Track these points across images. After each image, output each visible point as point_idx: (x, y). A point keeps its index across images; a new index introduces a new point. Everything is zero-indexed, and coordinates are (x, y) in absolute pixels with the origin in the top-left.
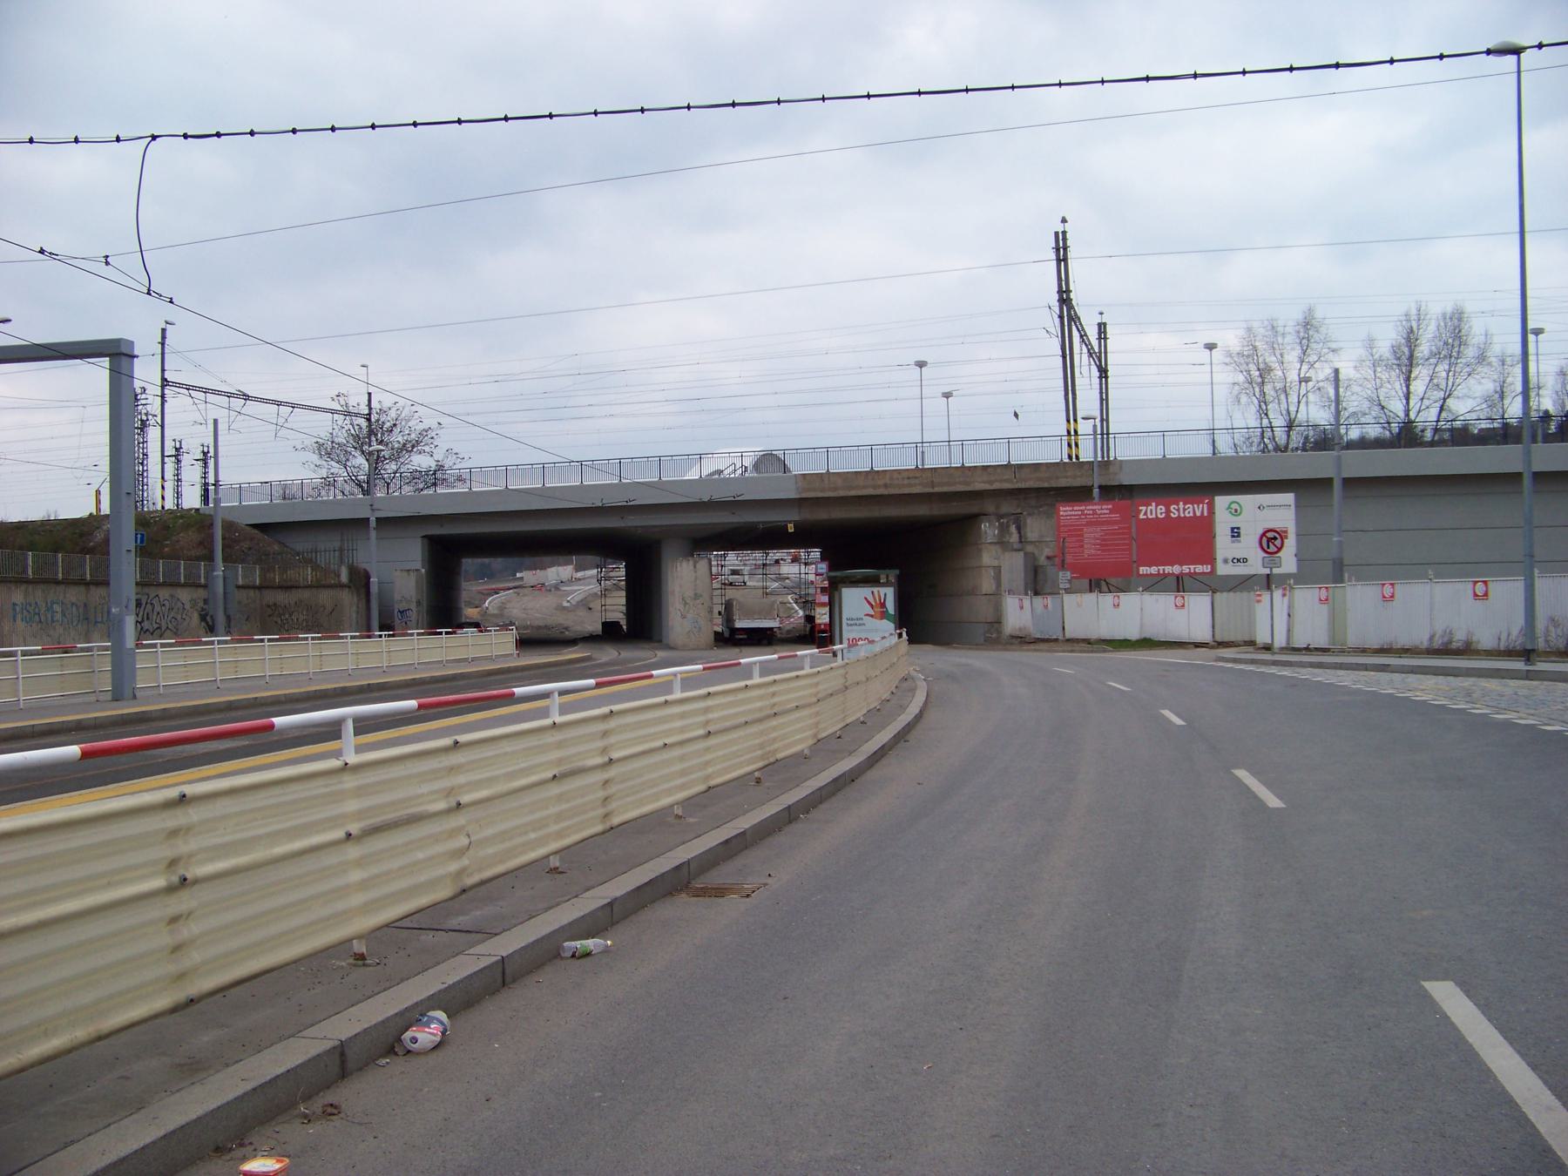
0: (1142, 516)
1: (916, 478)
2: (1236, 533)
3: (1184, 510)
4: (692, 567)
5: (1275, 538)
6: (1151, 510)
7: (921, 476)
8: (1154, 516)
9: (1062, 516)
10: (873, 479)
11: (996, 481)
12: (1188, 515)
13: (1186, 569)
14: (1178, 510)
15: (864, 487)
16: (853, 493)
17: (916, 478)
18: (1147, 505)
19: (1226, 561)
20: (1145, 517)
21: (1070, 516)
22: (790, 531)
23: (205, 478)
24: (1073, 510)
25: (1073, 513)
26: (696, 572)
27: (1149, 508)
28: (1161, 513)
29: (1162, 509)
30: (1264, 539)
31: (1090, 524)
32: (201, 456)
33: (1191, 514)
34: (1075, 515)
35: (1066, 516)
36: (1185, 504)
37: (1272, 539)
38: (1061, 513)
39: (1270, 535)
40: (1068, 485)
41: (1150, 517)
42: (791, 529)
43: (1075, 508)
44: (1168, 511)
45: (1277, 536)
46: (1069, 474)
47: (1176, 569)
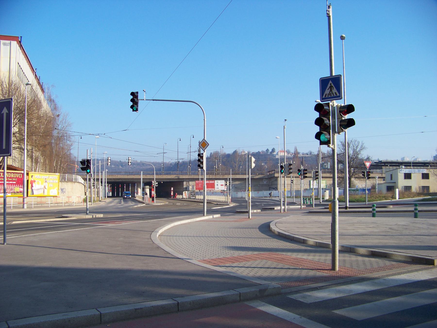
2: (217, 185)
13: (211, 189)
19: (216, 188)
31: (200, 183)
42: (162, 183)
44: (209, 182)
47: (210, 189)
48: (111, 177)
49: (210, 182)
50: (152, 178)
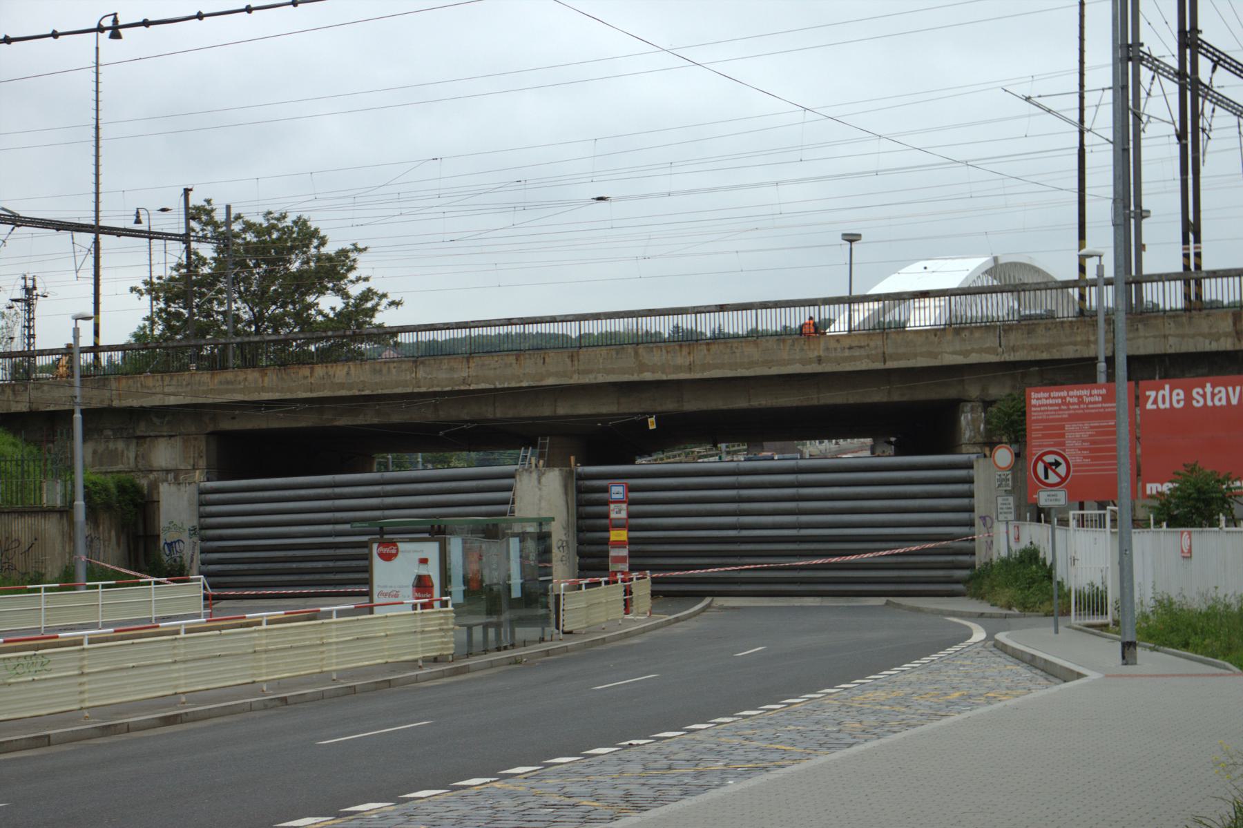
0: (1149, 406)
1: (860, 347)
3: (1213, 395)
4: (536, 483)
5: (1057, 464)
6: (1164, 396)
7: (868, 345)
8: (1167, 405)
9: (1035, 406)
10: (802, 350)
11: (973, 351)
12: (1217, 403)
14: (1204, 396)
15: (790, 362)
16: (775, 371)
17: (860, 347)
18: (1158, 388)
20: (1154, 407)
21: (1046, 405)
22: (651, 428)
23: (29, 327)
24: (1049, 397)
25: (1051, 401)
26: (540, 489)
27: (1161, 393)
28: (1178, 402)
29: (1179, 394)
30: (1040, 467)
31: (1074, 418)
32: (20, 294)
33: (1224, 402)
34: (1051, 405)
35: (1040, 406)
36: (1213, 387)
37: (1051, 464)
38: (1034, 402)
39: (1050, 459)
40: (1078, 355)
41: (1161, 406)
43: (1053, 394)
44: (1189, 398)
45: (1060, 460)
46: (1079, 339)
48: (271, 390)
49: (1198, 403)
50: (635, 378)
